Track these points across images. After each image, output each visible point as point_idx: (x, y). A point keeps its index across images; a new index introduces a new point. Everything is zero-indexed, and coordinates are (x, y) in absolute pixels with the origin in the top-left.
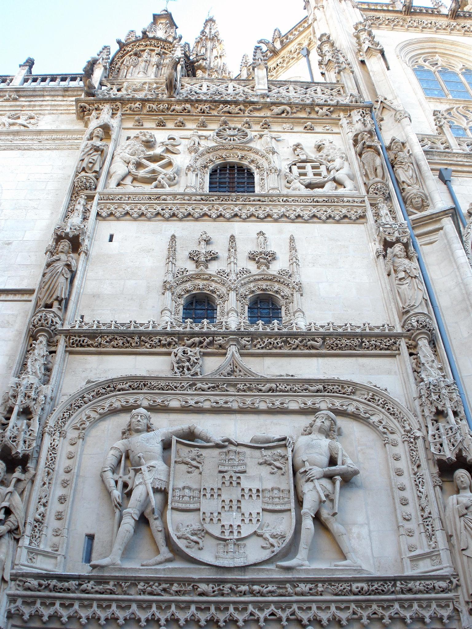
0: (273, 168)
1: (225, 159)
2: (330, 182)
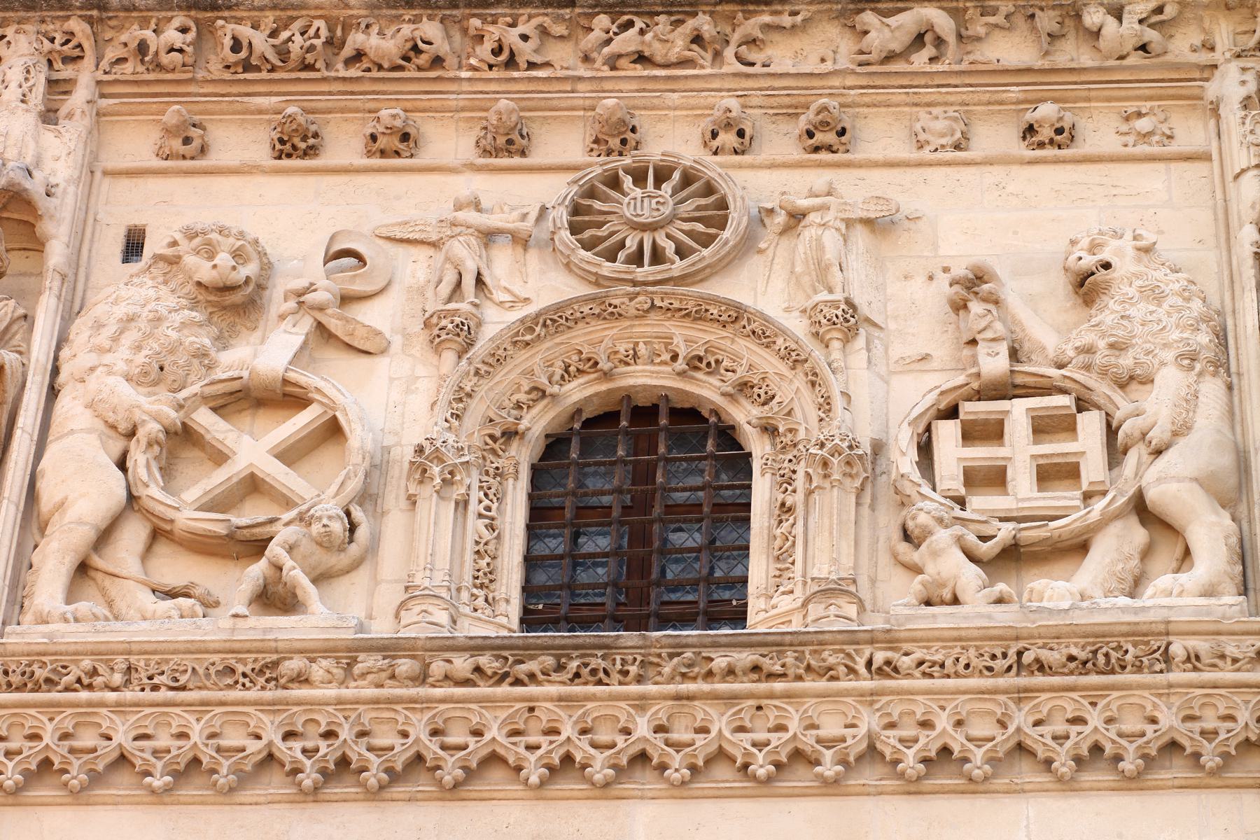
0: (836, 451)
1: (607, 376)
2: (1115, 528)
